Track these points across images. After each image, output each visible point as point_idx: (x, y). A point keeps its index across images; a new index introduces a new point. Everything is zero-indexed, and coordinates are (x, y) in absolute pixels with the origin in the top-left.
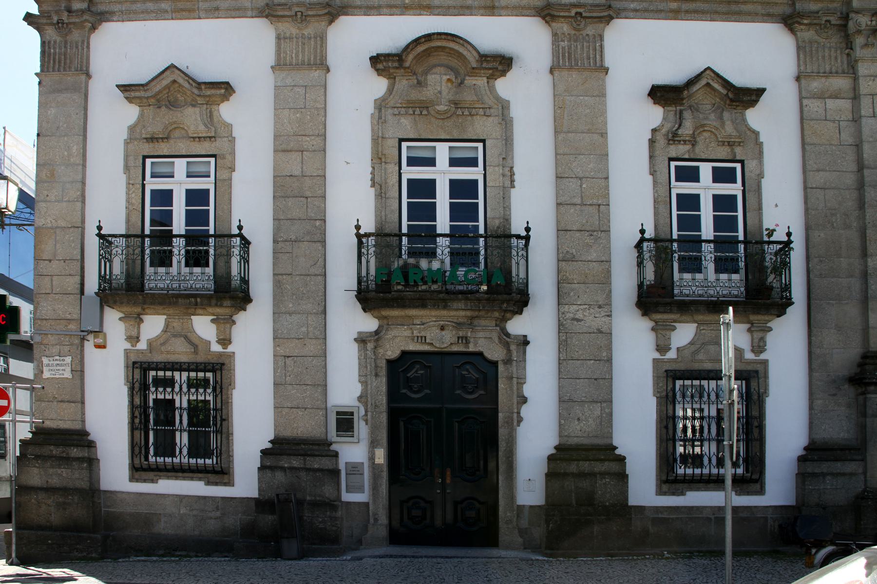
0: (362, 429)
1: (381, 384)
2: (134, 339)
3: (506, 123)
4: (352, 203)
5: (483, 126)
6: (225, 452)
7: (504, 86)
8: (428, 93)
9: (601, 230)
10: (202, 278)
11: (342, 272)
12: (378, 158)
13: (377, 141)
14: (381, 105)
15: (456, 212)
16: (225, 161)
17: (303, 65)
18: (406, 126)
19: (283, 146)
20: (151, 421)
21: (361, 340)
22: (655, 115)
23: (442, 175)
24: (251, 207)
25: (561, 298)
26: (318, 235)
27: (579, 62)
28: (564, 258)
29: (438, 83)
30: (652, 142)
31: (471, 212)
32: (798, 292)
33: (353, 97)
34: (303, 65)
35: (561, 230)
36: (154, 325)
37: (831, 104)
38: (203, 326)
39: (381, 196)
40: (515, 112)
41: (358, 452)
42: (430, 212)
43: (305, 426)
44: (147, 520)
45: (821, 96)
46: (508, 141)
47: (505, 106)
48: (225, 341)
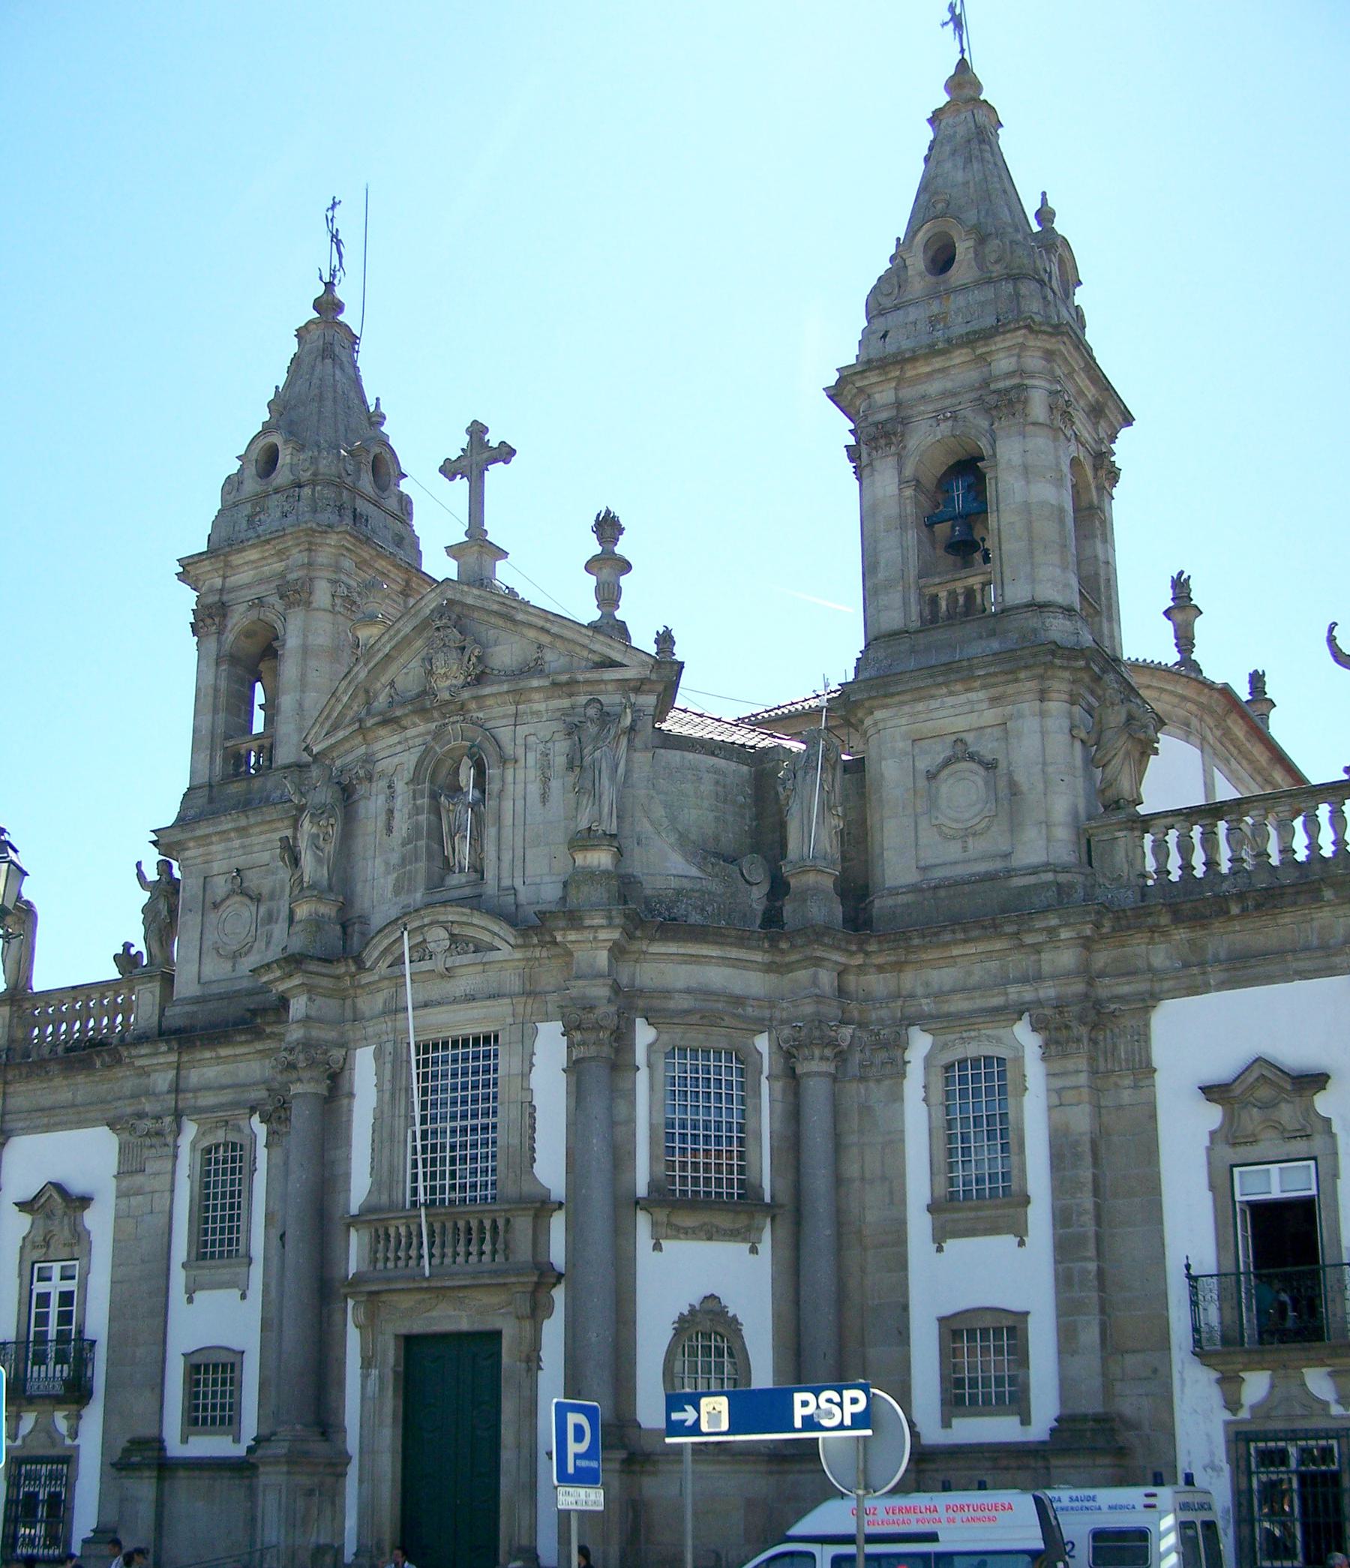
30: (22, 1248)
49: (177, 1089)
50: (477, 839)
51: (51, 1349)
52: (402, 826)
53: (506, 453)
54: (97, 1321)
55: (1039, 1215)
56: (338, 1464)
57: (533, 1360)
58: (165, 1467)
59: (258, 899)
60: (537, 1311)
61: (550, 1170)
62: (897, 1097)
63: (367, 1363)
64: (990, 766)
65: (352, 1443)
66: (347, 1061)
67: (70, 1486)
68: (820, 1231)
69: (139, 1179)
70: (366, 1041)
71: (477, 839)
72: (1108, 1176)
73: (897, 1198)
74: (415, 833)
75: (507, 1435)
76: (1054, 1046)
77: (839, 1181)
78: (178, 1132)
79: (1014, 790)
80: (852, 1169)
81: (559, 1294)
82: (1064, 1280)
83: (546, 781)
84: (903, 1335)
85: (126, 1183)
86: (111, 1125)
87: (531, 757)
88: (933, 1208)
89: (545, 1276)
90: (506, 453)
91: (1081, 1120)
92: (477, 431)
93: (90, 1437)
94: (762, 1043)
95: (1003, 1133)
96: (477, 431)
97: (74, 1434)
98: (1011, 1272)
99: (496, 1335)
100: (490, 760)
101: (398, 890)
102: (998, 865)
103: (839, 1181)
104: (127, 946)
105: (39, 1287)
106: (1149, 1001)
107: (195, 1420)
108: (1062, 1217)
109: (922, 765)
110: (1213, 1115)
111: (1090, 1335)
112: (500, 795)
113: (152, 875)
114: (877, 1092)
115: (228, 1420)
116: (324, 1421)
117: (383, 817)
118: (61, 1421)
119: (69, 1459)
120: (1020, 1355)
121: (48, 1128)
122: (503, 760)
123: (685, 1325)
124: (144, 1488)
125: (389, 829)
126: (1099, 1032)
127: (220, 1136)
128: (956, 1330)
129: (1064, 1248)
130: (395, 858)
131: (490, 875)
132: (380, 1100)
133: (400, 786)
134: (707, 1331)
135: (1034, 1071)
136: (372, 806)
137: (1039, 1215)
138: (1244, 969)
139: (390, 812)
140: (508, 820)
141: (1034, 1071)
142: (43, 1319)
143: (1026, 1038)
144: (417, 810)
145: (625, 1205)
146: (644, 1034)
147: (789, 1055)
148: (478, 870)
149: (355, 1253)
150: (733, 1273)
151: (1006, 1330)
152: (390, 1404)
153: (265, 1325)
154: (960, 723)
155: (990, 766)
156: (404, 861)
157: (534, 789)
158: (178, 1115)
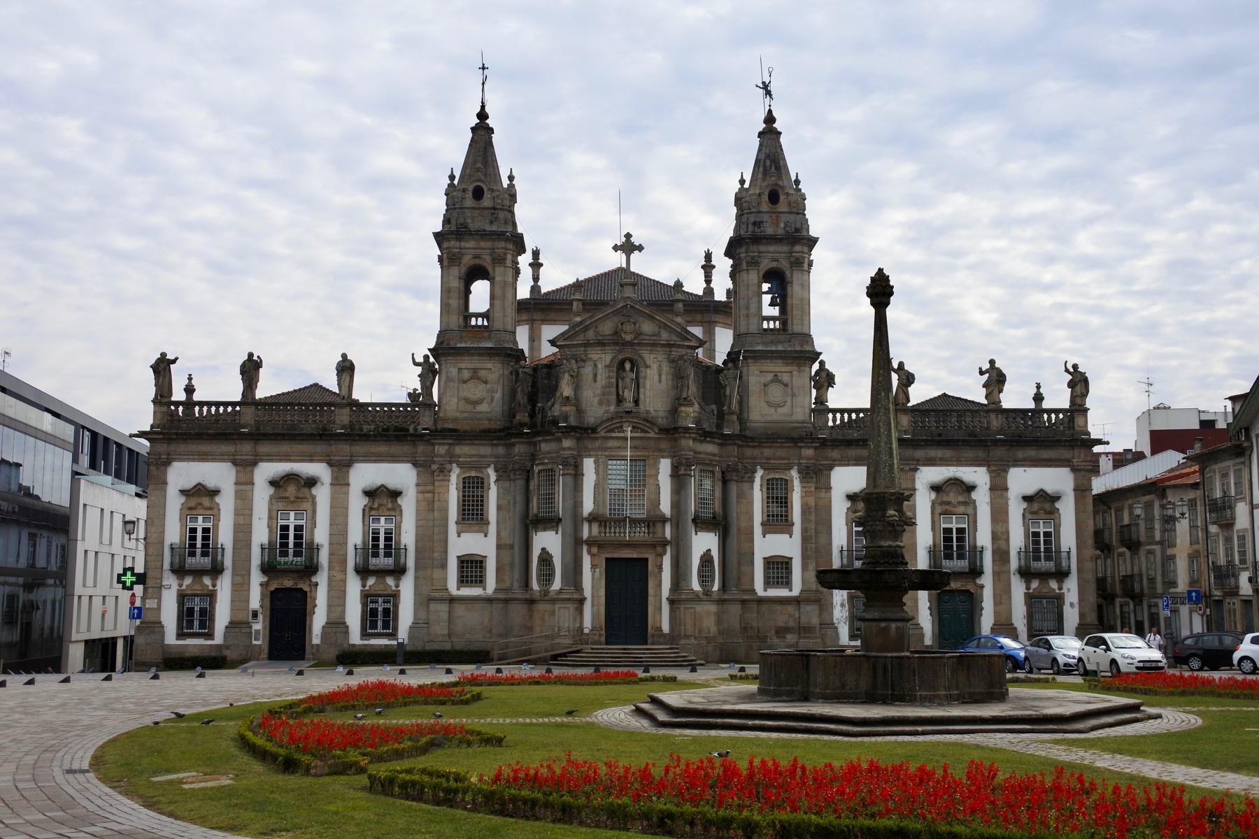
0: (260, 617)
1: (267, 601)
2: (180, 585)
3: (314, 504)
4: (261, 535)
5: (307, 505)
6: (212, 627)
7: (314, 491)
8: (287, 495)
9: (345, 543)
10: (207, 561)
11: (256, 559)
12: (270, 518)
13: (270, 511)
14: (271, 498)
15: (296, 537)
16: (217, 519)
17: (244, 485)
18: (280, 505)
19: (237, 513)
20: (185, 616)
21: (261, 585)
22: (365, 501)
23: (292, 522)
24: (225, 536)
25: (330, 568)
26: (249, 546)
28: (331, 554)
29: (291, 490)
31: (301, 537)
32: (411, 563)
33: (262, 495)
34: (244, 485)
35: (331, 544)
36: (188, 581)
37: (427, 495)
38: (207, 581)
39: (270, 531)
40: (318, 500)
41: (258, 626)
42: (287, 537)
43: (241, 617)
45: (423, 492)
46: (314, 512)
47: (314, 498)
48: (214, 586)
51: (382, 552)
53: (640, 248)
55: (797, 529)
56: (582, 601)
57: (660, 568)
58: (452, 600)
59: (486, 382)
61: (665, 507)
62: (752, 488)
63: (593, 566)
64: (786, 385)
65: (588, 592)
67: (396, 606)
68: (734, 531)
69: (430, 488)
70: (590, 456)
72: (818, 519)
73: (751, 519)
74: (608, 386)
75: (651, 591)
78: (450, 471)
79: (793, 395)
81: (668, 549)
83: (660, 375)
85: (421, 488)
86: (415, 465)
87: (655, 367)
88: (763, 524)
90: (640, 248)
92: (628, 236)
93: (407, 589)
95: (785, 502)
96: (628, 236)
97: (397, 586)
98: (788, 545)
99: (647, 560)
101: (600, 403)
102: (788, 418)
104: (415, 390)
105: (373, 526)
106: (831, 468)
107: (463, 581)
108: (804, 531)
109: (763, 380)
111: (812, 566)
112: (645, 378)
113: (420, 359)
114: (746, 486)
115: (480, 581)
116: (578, 586)
117: (591, 376)
119: (395, 596)
121: (375, 461)
122: (647, 367)
123: (702, 557)
124: (444, 608)
125: (595, 381)
126: (817, 476)
127: (473, 474)
128: (770, 563)
129: (805, 539)
130: (599, 392)
131: (641, 406)
132: (598, 479)
133: (600, 366)
135: (797, 484)
136: (587, 370)
137: (797, 529)
139: (595, 376)
140: (648, 386)
141: (797, 484)
143: (794, 473)
144: (609, 377)
147: (723, 473)
148: (636, 402)
150: (704, 543)
153: (499, 547)
154: (777, 369)
156: (603, 394)
157: (656, 377)
158: (451, 462)
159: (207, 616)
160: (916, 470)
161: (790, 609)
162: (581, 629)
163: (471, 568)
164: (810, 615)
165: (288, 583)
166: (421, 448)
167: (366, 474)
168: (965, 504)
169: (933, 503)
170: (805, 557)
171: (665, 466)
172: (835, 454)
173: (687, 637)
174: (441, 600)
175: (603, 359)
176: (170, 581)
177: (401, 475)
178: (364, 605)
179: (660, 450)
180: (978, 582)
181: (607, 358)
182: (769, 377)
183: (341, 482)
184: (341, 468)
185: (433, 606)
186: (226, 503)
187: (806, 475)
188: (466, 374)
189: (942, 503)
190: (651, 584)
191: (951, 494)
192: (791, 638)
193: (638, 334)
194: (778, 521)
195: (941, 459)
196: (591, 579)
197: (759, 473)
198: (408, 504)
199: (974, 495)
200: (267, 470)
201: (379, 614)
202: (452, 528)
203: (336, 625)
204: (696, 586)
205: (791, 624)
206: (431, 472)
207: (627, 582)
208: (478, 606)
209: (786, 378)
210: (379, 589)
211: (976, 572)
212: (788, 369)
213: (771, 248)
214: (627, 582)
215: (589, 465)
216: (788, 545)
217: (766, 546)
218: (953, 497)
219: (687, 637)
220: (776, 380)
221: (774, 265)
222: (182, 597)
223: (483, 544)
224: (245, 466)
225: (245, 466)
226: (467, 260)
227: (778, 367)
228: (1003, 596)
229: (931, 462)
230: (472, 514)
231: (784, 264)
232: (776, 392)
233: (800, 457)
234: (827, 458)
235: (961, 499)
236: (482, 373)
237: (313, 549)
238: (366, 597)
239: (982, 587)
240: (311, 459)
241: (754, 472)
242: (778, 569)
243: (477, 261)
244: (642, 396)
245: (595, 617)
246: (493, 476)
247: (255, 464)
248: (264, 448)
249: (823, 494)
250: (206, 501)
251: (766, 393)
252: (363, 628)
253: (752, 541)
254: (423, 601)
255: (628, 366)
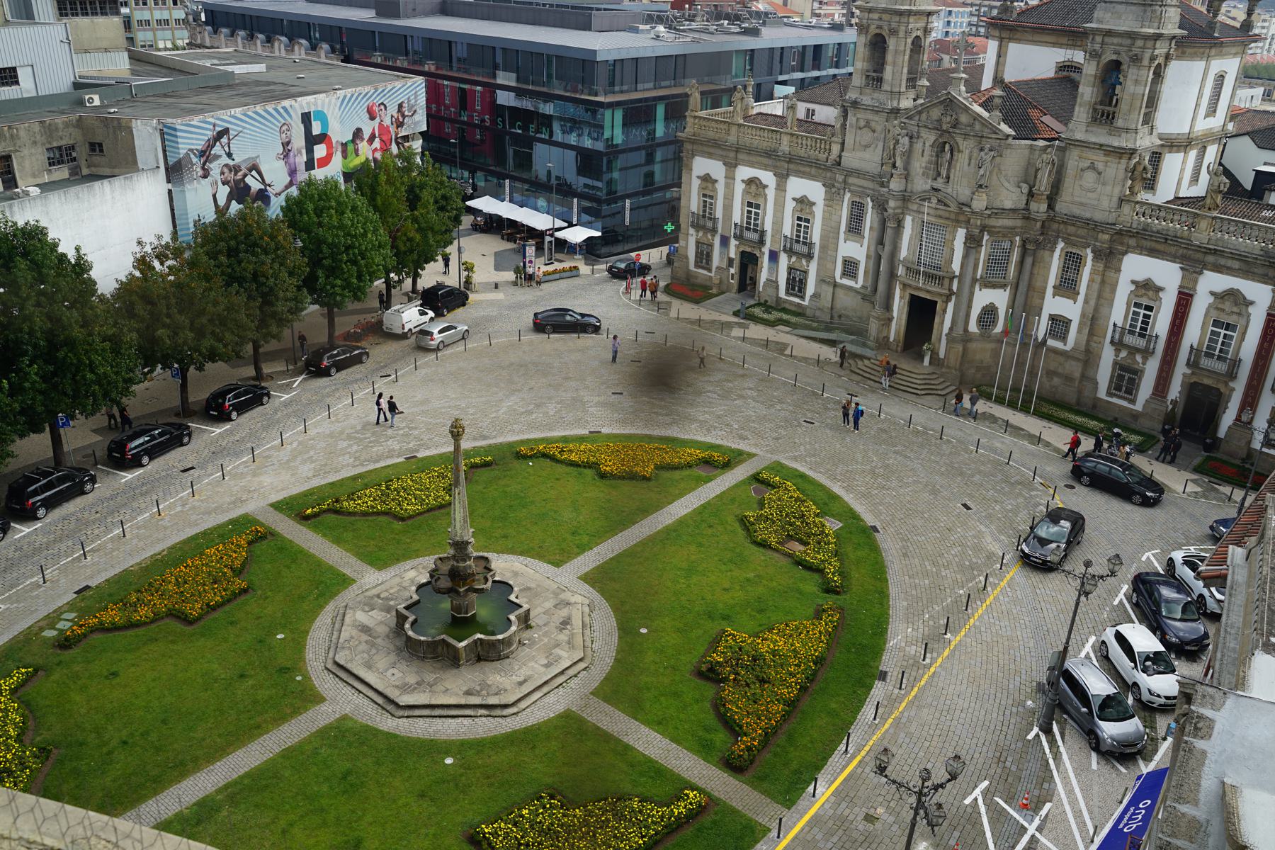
27: (781, 188)
29: (753, 187)
34: (730, 178)
44: (696, 278)
47: (766, 195)
49: (845, 182)
50: (949, 170)
52: (926, 158)
54: (816, 237)
56: (890, 320)
57: (945, 311)
58: (835, 285)
60: (948, 299)
64: (1100, 173)
65: (895, 314)
66: (903, 219)
71: (949, 170)
74: (930, 162)
75: (936, 326)
76: (1095, 258)
77: (1031, 273)
80: (1035, 272)
81: (953, 298)
82: (1083, 315)
84: (1040, 316)
88: (1054, 287)
89: (951, 293)
91: (1098, 278)
94: (1018, 238)
98: (1071, 309)
100: (955, 149)
103: (1031, 273)
106: (1126, 253)
107: (844, 274)
108: (1086, 301)
110: (1133, 287)
114: (1047, 253)
118: (804, 262)
119: (806, 272)
120: (1067, 331)
128: (1053, 318)
134: (989, 313)
136: (918, 146)
138: (1153, 253)
142: (799, 231)
143: (1089, 251)
145: (974, 281)
146: (986, 237)
147: (1024, 243)
149: (901, 271)
151: (1067, 322)
152: (906, 310)
153: (868, 257)
155: (1100, 173)
157: (967, 161)
159: (709, 257)
160: (1201, 273)
161: (1062, 359)
162: (887, 338)
163: (850, 267)
164: (1075, 369)
165: (748, 250)
166: (829, 175)
167: (799, 186)
168: (1240, 314)
169: (1210, 306)
170: (1081, 324)
171: (961, 233)
172: (1132, 242)
173: (948, 367)
174: (829, 283)
175: (930, 137)
176: (692, 231)
177: (814, 190)
178: (789, 274)
179: (957, 221)
180: (1231, 384)
181: (932, 138)
182: (1087, 164)
183: (781, 188)
184: (782, 178)
185: (824, 287)
186: (720, 188)
187: (1097, 255)
188: (862, 123)
189: (1217, 308)
190: (937, 320)
191: (1228, 304)
192: (1056, 381)
193: (955, 125)
194: (1067, 287)
195: (1228, 268)
196: (899, 306)
197: (1061, 245)
198: (819, 211)
199: (1251, 309)
200: (744, 172)
201: (796, 283)
202: (842, 236)
203: (773, 283)
204: (973, 327)
205: (1060, 370)
206: (833, 194)
207: (922, 313)
208: (852, 294)
209: (1100, 166)
210: (797, 266)
211: (1232, 375)
212: (1104, 159)
213: (1115, 40)
214: (922, 313)
215: (908, 221)
216: (1071, 309)
217: (1054, 305)
218: (1227, 306)
219: (948, 367)
220: (1092, 167)
221: (1114, 57)
222: (698, 243)
223: (856, 250)
224: (731, 166)
225: (731, 166)
226: (873, 30)
227: (1098, 158)
228: (1250, 401)
229: (1218, 269)
230: (855, 228)
231: (1124, 58)
232: (1090, 177)
233: (1096, 240)
234: (1122, 244)
235: (1235, 309)
236: (873, 124)
237: (763, 233)
238: (790, 269)
239: (1233, 389)
240: (765, 168)
241: (1056, 243)
242: (1059, 325)
243: (878, 31)
244: (952, 176)
245: (897, 332)
246: (870, 204)
247: (736, 166)
248: (741, 156)
249: (1111, 274)
250: (710, 185)
251: (1081, 177)
252: (787, 289)
253: (1043, 299)
254: (821, 281)
255: (947, 147)
